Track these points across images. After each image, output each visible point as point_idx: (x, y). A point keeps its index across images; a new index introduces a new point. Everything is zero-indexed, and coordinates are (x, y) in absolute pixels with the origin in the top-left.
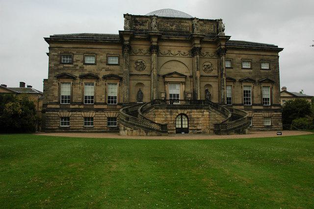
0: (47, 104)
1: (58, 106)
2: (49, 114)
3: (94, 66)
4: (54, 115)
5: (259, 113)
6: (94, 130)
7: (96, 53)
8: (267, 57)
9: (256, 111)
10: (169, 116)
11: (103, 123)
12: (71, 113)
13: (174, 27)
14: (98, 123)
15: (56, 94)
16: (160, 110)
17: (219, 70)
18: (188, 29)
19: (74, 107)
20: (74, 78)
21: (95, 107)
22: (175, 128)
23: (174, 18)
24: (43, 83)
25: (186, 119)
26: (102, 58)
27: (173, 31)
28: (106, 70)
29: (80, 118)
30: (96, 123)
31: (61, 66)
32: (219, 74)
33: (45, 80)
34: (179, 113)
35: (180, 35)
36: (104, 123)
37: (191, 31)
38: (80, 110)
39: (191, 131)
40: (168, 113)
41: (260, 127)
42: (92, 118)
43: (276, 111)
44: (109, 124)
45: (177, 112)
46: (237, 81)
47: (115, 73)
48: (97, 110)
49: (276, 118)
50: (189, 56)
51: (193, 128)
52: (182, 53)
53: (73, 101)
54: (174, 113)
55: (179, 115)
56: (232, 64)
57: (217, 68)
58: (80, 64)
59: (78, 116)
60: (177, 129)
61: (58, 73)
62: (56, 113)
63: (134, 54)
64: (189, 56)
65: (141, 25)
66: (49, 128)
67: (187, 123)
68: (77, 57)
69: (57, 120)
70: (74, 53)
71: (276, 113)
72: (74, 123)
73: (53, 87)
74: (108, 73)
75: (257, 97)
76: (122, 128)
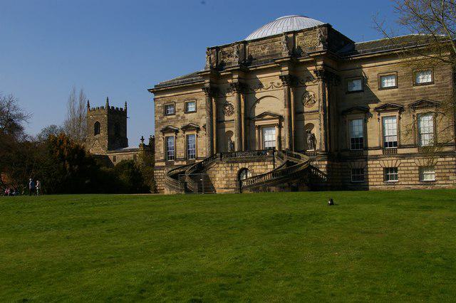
5: (409, 161)
9: (404, 156)
10: (230, 172)
13: (266, 51)
16: (221, 165)
20: (177, 131)
23: (265, 38)
31: (165, 119)
34: (240, 168)
40: (229, 168)
41: (410, 183)
49: (442, 167)
52: (276, 85)
58: (182, 113)
61: (162, 127)
65: (229, 56)
71: (443, 159)
73: (159, 142)
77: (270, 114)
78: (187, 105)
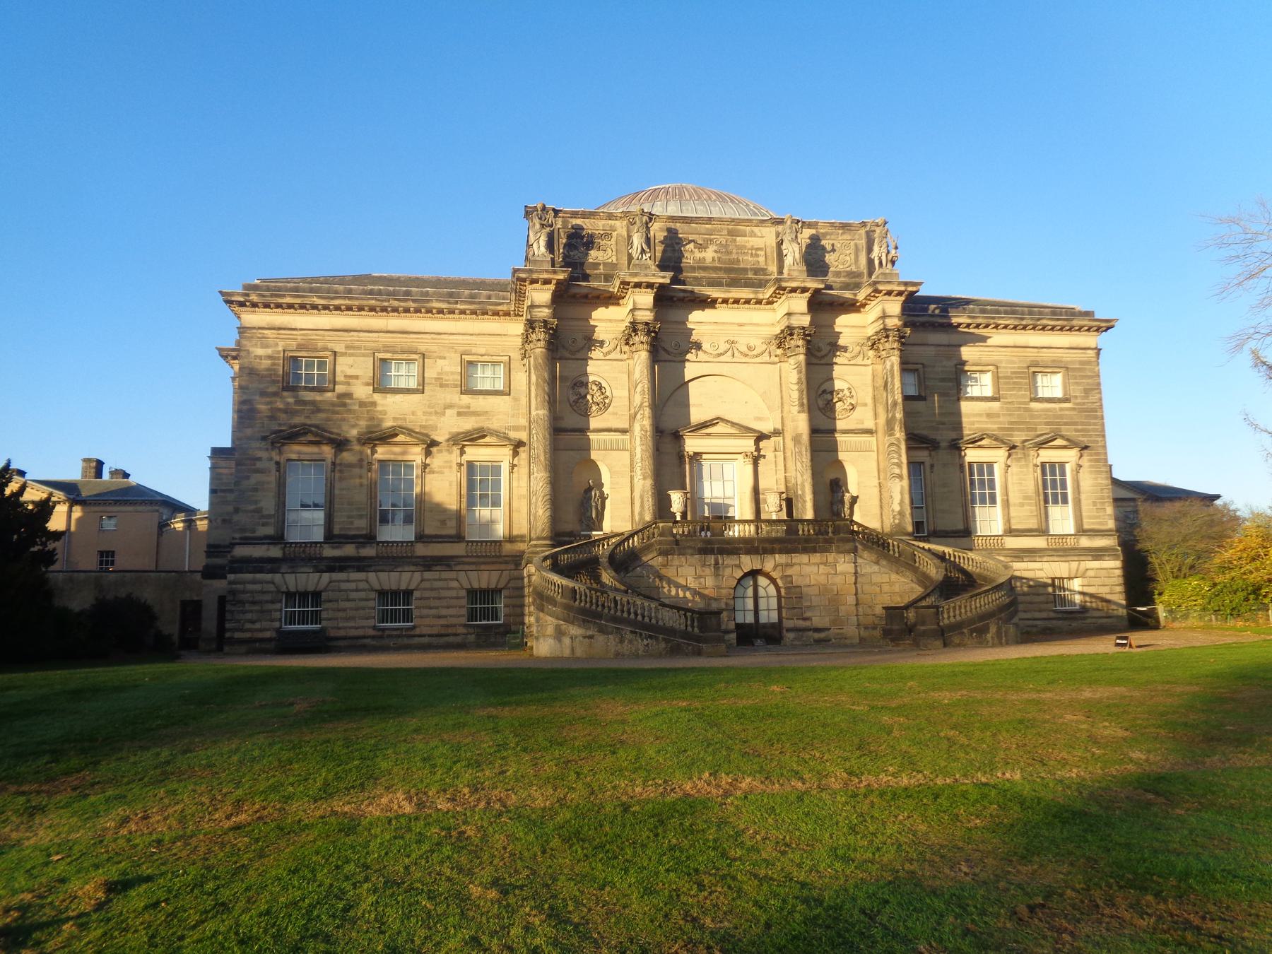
0: (232, 545)
1: (275, 552)
2: (243, 583)
3: (418, 396)
4: (257, 587)
6: (417, 640)
7: (422, 348)
8: (1058, 353)
12: (326, 577)
14: (433, 612)
15: (268, 505)
17: (881, 410)
18: (762, 259)
19: (337, 553)
21: (421, 550)
22: (732, 626)
24: (208, 463)
25: (772, 590)
26: (447, 369)
27: (705, 269)
28: (459, 414)
29: (363, 595)
30: (425, 612)
32: (882, 420)
33: (217, 453)
35: (734, 283)
36: (457, 614)
37: (773, 268)
38: (360, 564)
39: (791, 635)
41: (1037, 615)
42: (408, 593)
43: (1097, 554)
44: (472, 615)
45: (739, 566)
46: (943, 444)
47: (494, 424)
48: (429, 563)
50: (766, 358)
51: (801, 624)
52: (744, 349)
53: (336, 531)
54: (728, 572)
55: (746, 575)
57: (869, 401)
59: (353, 586)
60: (738, 625)
62: (269, 576)
63: (568, 355)
64: (766, 358)
66: (237, 635)
69: (270, 607)
70: (339, 348)
71: (1096, 564)
72: (341, 614)
73: (255, 478)
74: (468, 424)
75: (1022, 505)
76: (550, 630)
77: (733, 424)
78: (382, 365)
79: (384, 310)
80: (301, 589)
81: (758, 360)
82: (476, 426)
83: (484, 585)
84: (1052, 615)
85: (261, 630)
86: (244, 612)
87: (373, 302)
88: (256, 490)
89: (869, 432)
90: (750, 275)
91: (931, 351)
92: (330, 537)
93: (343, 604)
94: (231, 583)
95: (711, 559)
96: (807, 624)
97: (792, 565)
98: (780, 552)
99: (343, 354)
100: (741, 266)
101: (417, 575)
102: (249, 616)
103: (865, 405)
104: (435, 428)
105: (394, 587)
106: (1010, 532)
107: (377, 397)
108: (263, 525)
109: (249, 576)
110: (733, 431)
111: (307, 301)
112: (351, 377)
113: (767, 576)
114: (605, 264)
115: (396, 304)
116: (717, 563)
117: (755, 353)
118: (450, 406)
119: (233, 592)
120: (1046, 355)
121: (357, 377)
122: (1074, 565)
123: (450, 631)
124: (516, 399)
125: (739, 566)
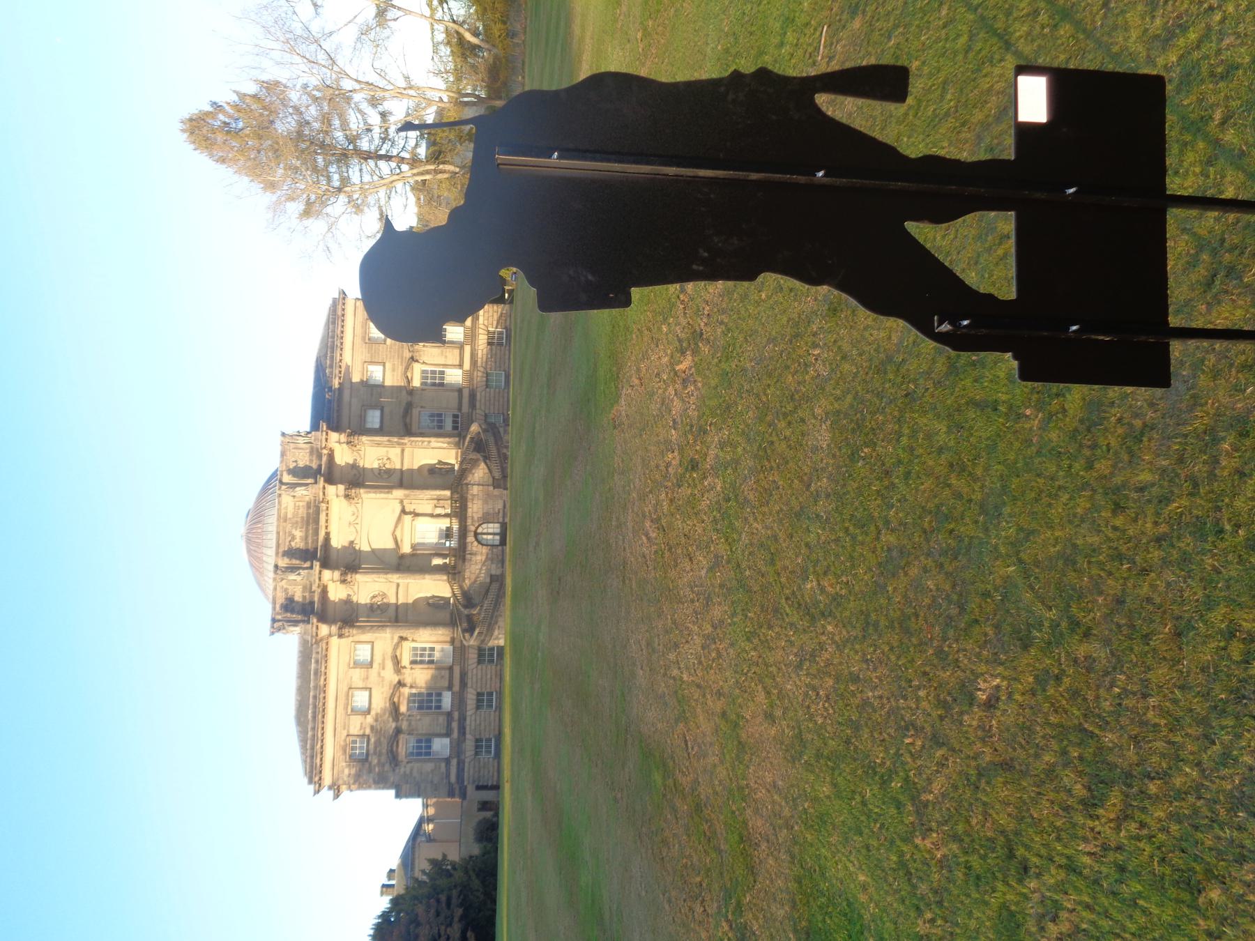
1: (454, 762)
3: (373, 691)
7: (345, 689)
11: (489, 672)
12: (468, 736)
14: (489, 682)
18: (301, 504)
21: (456, 688)
24: (404, 800)
25: (484, 526)
27: (306, 537)
28: (383, 669)
29: (478, 718)
30: (488, 686)
33: (398, 796)
34: (474, 539)
35: (317, 521)
36: (490, 669)
38: (462, 719)
41: (507, 357)
44: (491, 661)
45: (472, 543)
46: (409, 399)
47: (389, 651)
51: (501, 514)
54: (474, 549)
55: (477, 540)
56: (374, 407)
59: (473, 723)
62: (466, 765)
63: (355, 614)
66: (495, 778)
67: (491, 525)
68: (355, 727)
69: (482, 763)
73: (415, 774)
74: (389, 665)
75: (446, 357)
77: (396, 527)
78: (355, 711)
79: (324, 710)
80: (473, 748)
81: (360, 510)
82: (390, 660)
83: (476, 656)
84: (507, 348)
85: (493, 766)
86: (484, 776)
87: (320, 716)
88: (421, 773)
89: (403, 451)
90: (311, 511)
91: (354, 401)
92: (448, 735)
93: (482, 727)
94: (469, 783)
95: (468, 557)
96: (501, 511)
97: (473, 517)
98: (466, 522)
99: (348, 731)
100: (305, 515)
101: (470, 690)
102: (486, 773)
103: (387, 452)
104: (391, 681)
105: (475, 702)
106: (461, 366)
107: (373, 713)
108: (440, 768)
109: (466, 774)
110: (399, 527)
111: (319, 751)
112: (361, 726)
113: (477, 528)
114: (303, 592)
115: (321, 704)
116: (470, 554)
117: (356, 511)
118: (379, 674)
119: (474, 782)
120: (359, 331)
121: (362, 724)
122: (481, 331)
123: (498, 673)
124: (376, 638)
125: (472, 543)
